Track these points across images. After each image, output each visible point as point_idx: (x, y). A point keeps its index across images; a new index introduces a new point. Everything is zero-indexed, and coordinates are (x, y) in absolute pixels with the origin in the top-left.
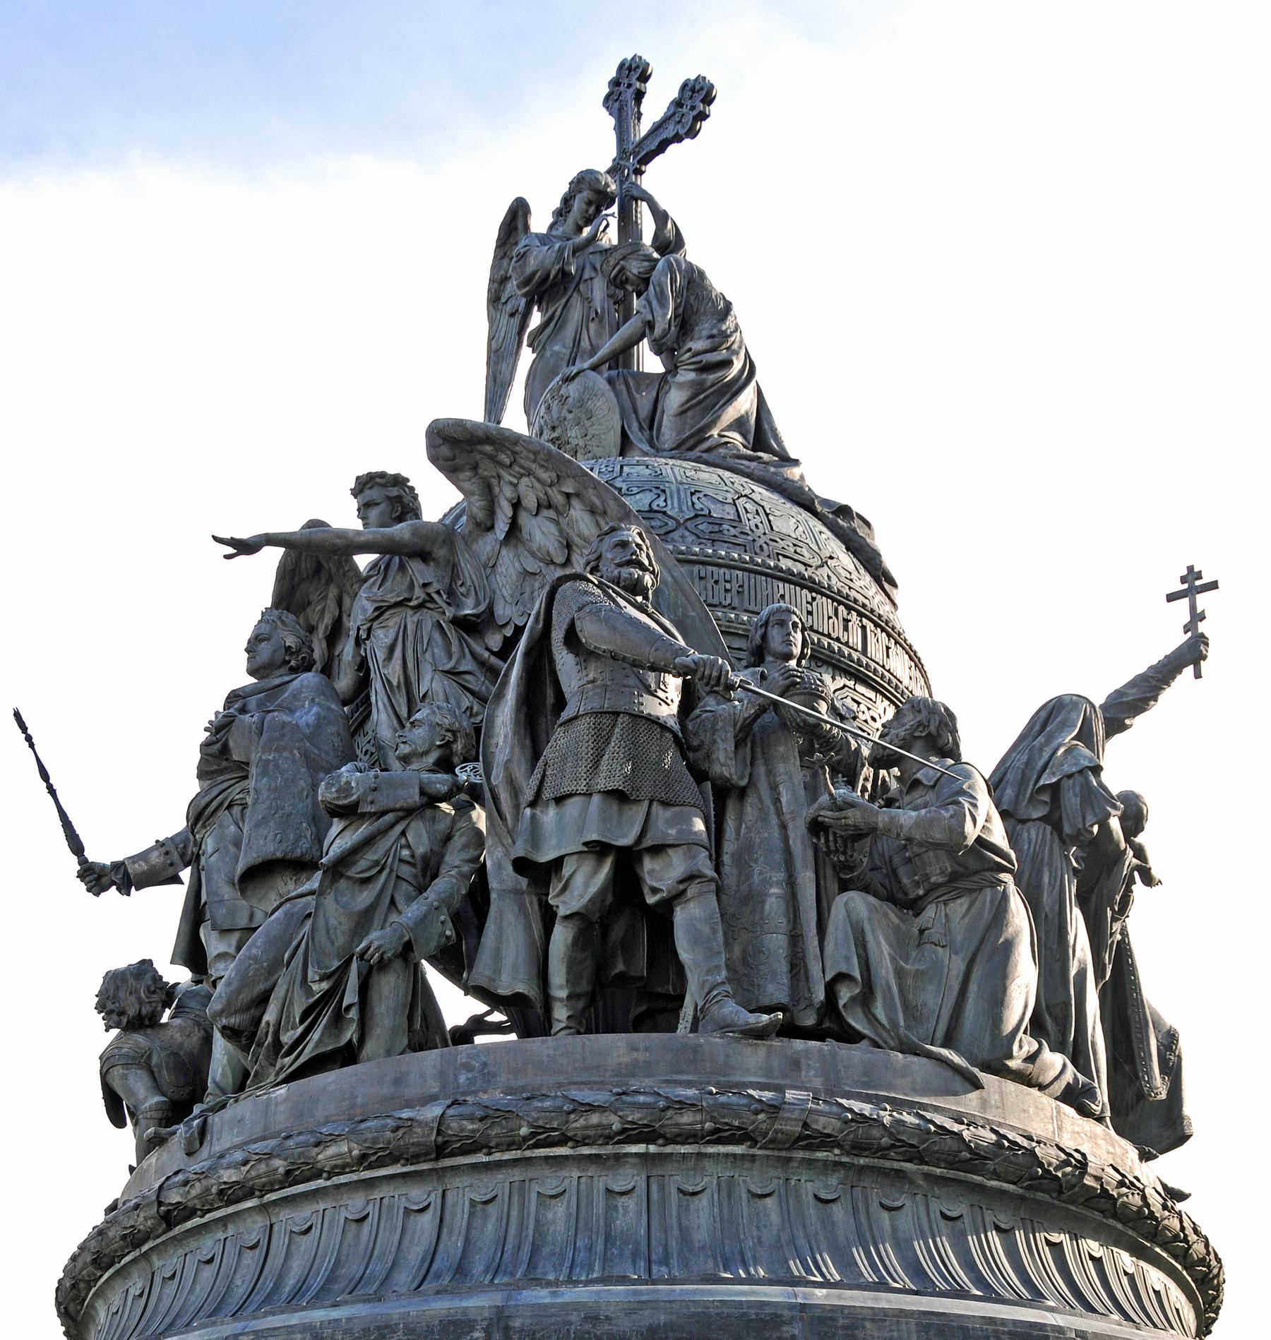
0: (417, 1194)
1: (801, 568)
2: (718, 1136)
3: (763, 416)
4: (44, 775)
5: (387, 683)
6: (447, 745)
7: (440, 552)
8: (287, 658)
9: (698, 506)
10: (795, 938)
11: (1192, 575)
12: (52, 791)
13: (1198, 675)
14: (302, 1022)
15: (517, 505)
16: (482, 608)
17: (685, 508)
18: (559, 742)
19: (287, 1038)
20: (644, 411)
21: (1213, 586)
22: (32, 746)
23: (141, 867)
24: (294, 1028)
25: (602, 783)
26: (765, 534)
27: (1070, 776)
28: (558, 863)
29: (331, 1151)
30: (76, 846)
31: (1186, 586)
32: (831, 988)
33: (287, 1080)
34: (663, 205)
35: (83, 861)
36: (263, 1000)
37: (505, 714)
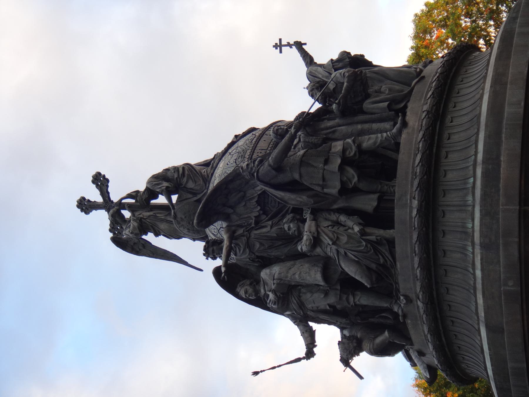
1: (256, 138)
3: (198, 164)
4: (274, 368)
5: (270, 247)
6: (298, 220)
7: (233, 228)
8: (253, 285)
9: (232, 163)
11: (276, 46)
13: (305, 44)
17: (233, 166)
19: (382, 261)
20: (190, 196)
21: (280, 40)
22: (264, 371)
23: (309, 339)
24: (379, 259)
25: (321, 165)
26: (244, 146)
27: (333, 66)
28: (342, 183)
30: (298, 360)
31: (279, 48)
32: (390, 110)
34: (124, 195)
35: (304, 358)
36: (369, 269)
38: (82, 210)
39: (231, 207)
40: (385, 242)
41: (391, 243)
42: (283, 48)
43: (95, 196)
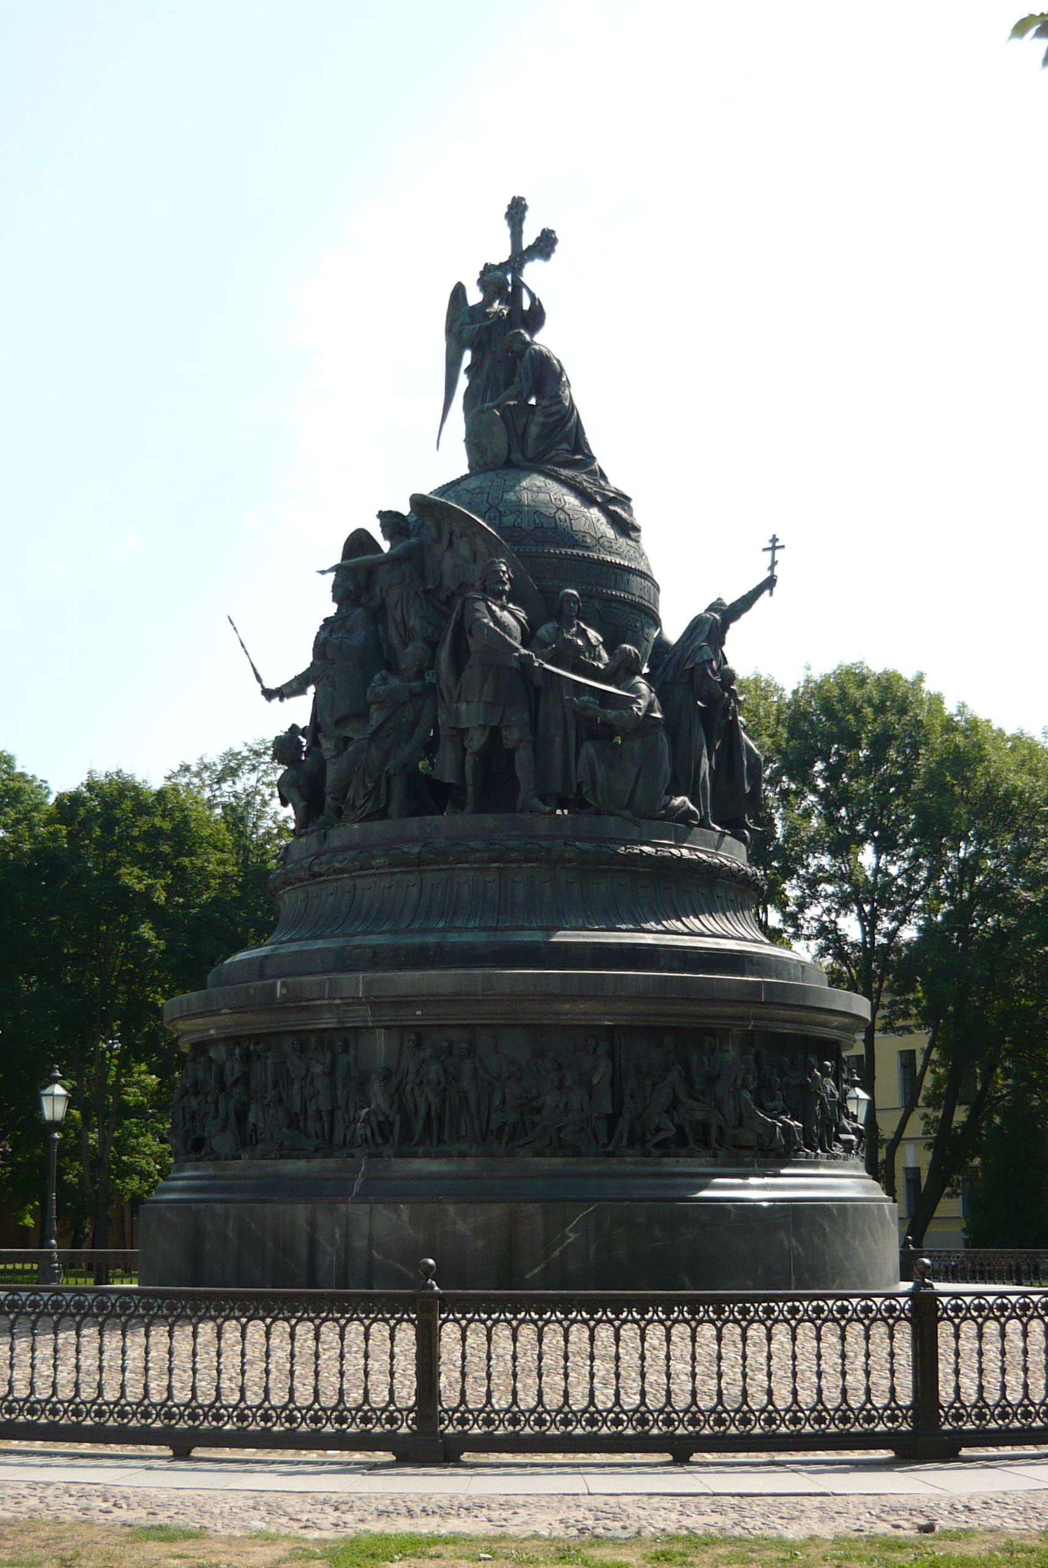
0: (411, 878)
2: (527, 861)
10: (566, 760)
11: (774, 539)
12: (247, 653)
13: (771, 594)
14: (365, 795)
15: (451, 534)
16: (437, 584)
18: (467, 674)
21: (783, 547)
27: (699, 664)
28: (468, 729)
29: (377, 861)
30: (259, 679)
31: (770, 545)
32: (579, 787)
33: (360, 821)
35: (263, 687)
36: (346, 788)
37: (444, 653)
38: (510, 207)
39: (450, 544)
40: (382, 805)
41: (382, 814)
42: (770, 553)
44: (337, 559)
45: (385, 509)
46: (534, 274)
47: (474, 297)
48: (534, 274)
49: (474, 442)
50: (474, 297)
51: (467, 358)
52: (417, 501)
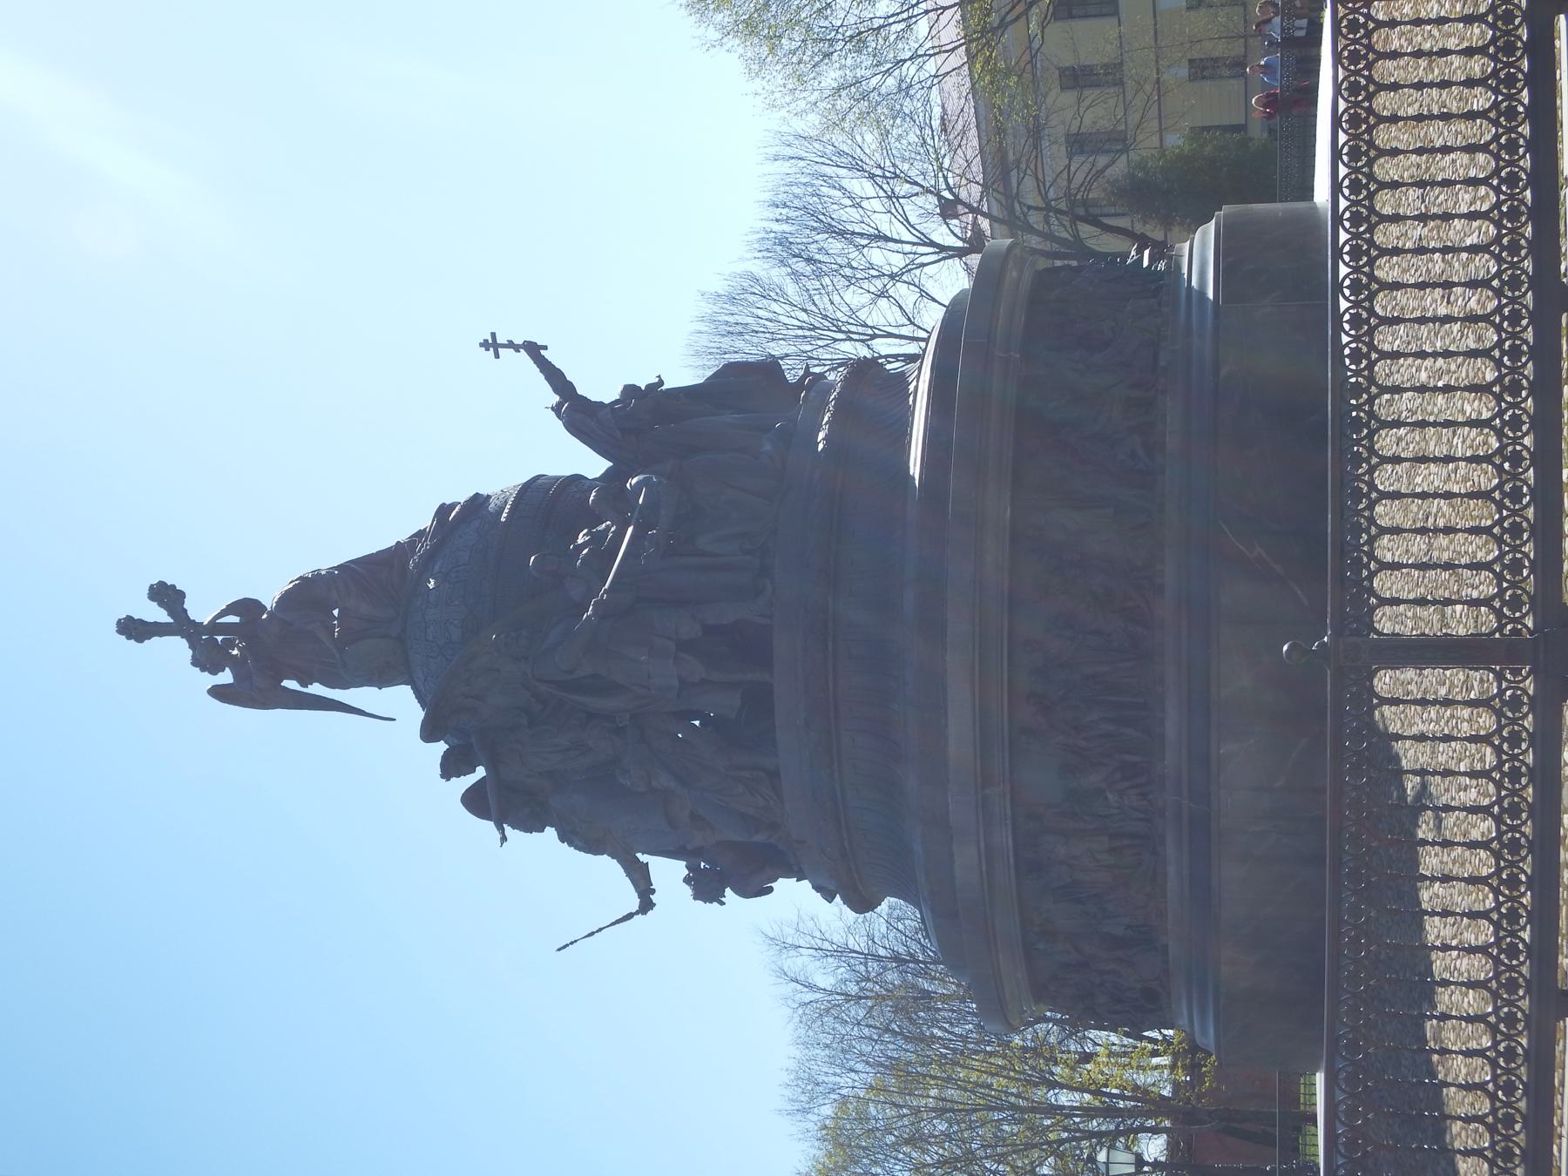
11: (485, 345)
12: (600, 930)
13: (545, 348)
21: (493, 335)
22: (576, 941)
30: (629, 916)
31: (491, 349)
35: (637, 913)
41: (774, 775)
43: (157, 614)
44: (489, 826)
45: (439, 771)
46: (201, 610)
47: (226, 677)
48: (201, 610)
49: (381, 679)
50: (226, 677)
51: (291, 684)
52: (430, 732)
